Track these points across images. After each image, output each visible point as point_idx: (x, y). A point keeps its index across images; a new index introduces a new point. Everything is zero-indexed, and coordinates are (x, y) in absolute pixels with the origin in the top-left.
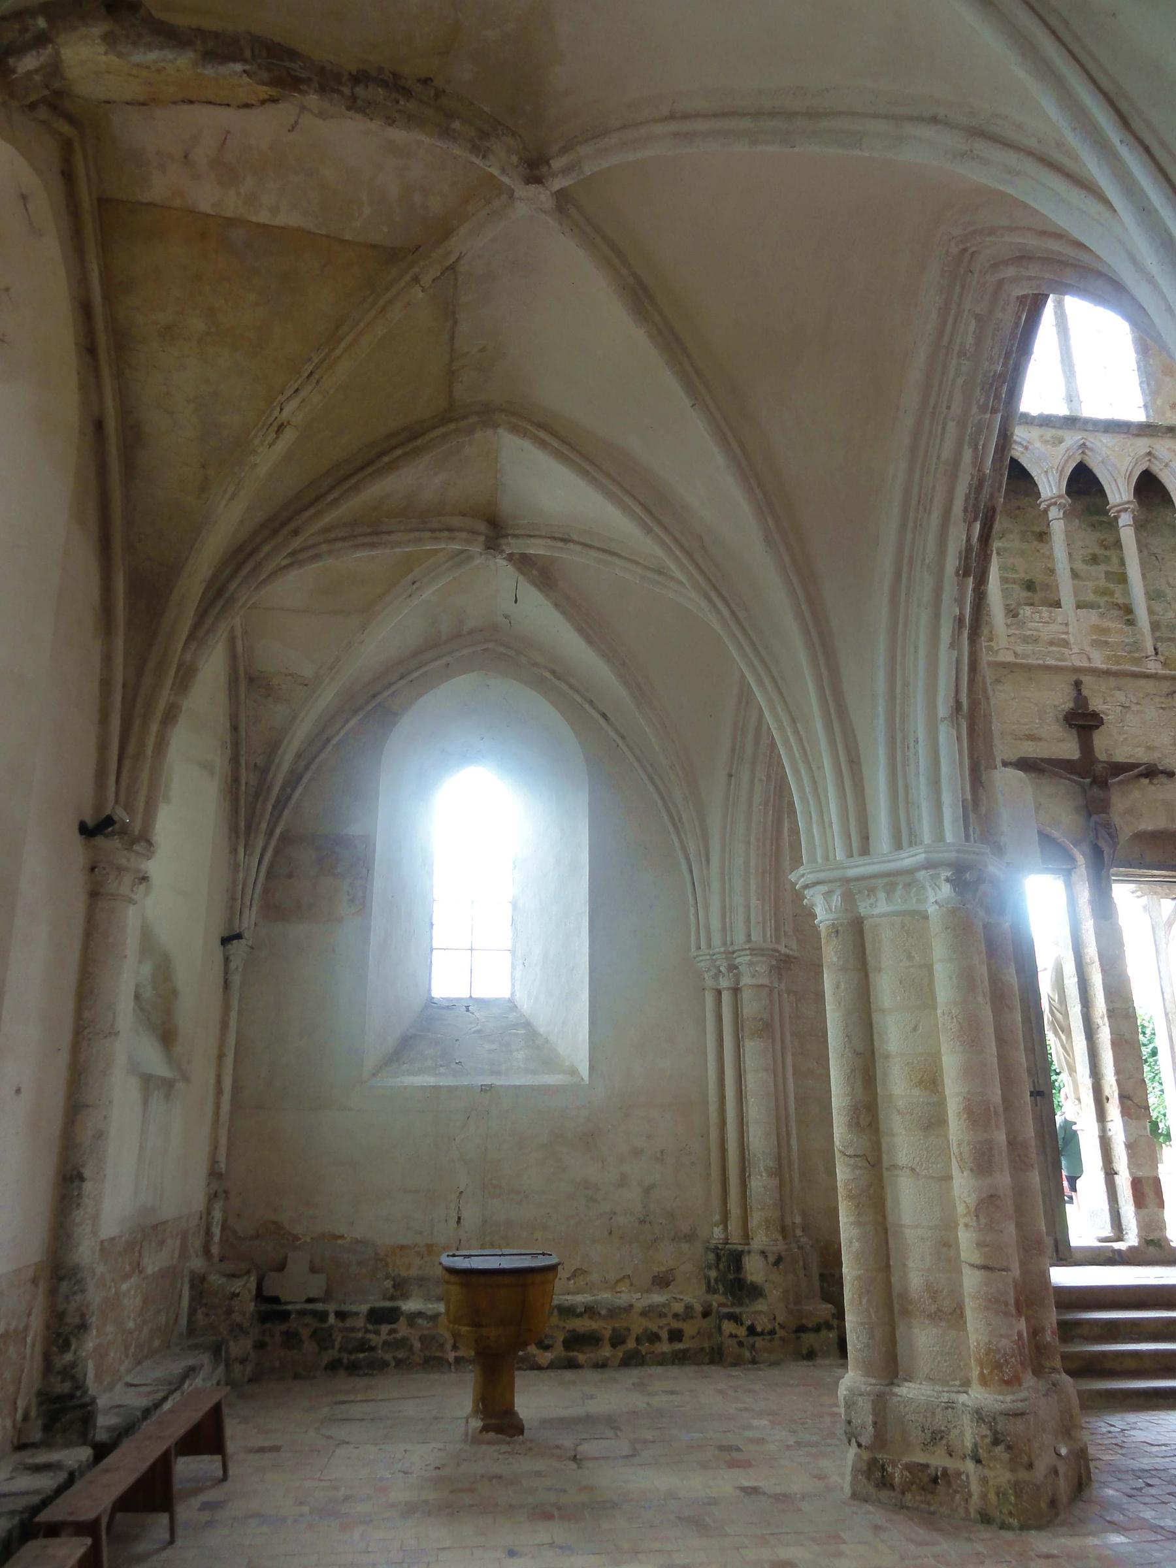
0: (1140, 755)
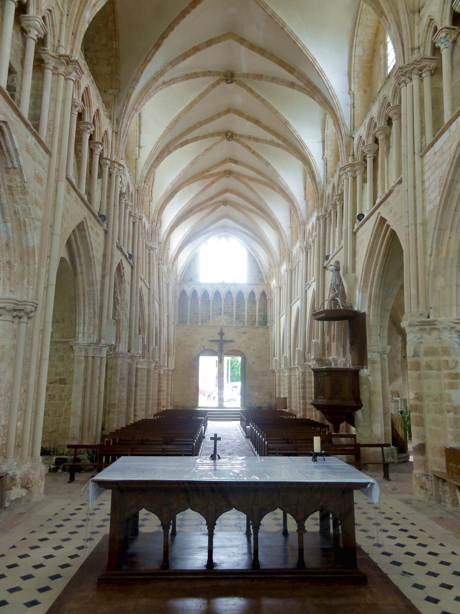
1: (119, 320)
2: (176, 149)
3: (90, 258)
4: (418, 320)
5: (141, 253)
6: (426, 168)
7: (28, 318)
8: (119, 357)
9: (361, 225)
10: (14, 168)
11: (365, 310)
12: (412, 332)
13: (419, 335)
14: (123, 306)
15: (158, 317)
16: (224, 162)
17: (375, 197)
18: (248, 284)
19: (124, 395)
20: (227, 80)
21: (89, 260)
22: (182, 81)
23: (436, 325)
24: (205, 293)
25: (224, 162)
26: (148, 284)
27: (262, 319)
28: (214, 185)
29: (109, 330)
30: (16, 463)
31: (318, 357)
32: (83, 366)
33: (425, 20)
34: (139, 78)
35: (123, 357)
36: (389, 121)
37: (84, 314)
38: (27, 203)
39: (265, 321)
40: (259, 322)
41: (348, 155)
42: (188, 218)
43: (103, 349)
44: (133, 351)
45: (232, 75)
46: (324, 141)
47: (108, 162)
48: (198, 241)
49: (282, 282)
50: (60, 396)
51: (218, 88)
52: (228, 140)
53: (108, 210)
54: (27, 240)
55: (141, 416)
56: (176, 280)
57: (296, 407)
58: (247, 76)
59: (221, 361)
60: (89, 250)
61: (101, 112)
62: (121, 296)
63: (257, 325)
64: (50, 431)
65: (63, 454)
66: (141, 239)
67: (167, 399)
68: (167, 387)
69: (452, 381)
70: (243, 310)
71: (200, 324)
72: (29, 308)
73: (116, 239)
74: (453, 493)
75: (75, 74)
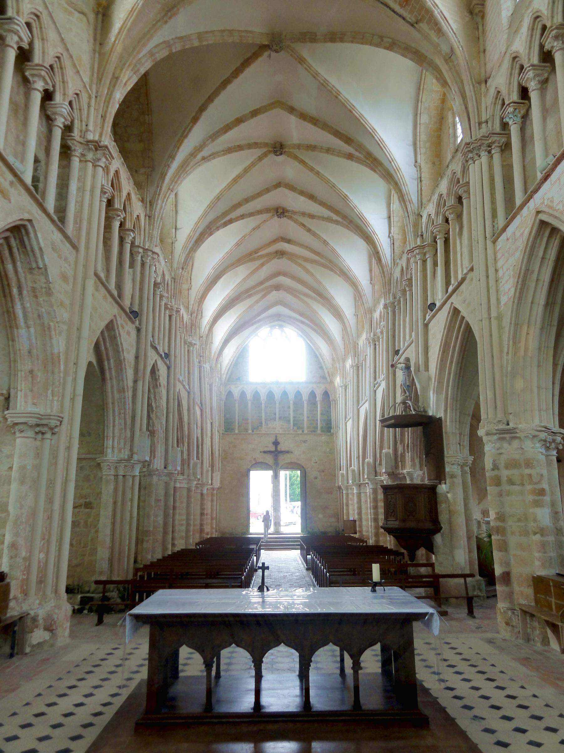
0: (287, 449)
1: (154, 431)
2: (218, 230)
3: (120, 361)
4: (496, 428)
5: (179, 351)
6: (499, 255)
7: (53, 434)
8: (154, 474)
9: (433, 316)
10: (39, 268)
11: (440, 414)
12: (490, 441)
13: (498, 445)
14: (158, 414)
15: (199, 425)
16: (275, 241)
17: (448, 283)
18: (306, 383)
19: (160, 519)
20: (275, 152)
21: (120, 364)
22: (224, 155)
23: (516, 433)
24: (256, 395)
25: (275, 241)
26: (187, 387)
27: (324, 424)
28: (265, 268)
29: (142, 443)
30: (38, 602)
31: (390, 470)
32: (112, 487)
33: (492, 92)
34: (175, 156)
35: (159, 475)
36: (460, 200)
37: (114, 426)
38: (51, 306)
39: (329, 428)
40: (322, 428)
41: (416, 236)
42: (234, 306)
43: (136, 466)
44: (170, 467)
45: (282, 146)
46: (389, 217)
47: (141, 250)
48: (246, 332)
49: (348, 380)
50: (86, 522)
51: (266, 160)
52: (279, 217)
53: (141, 304)
54: (52, 346)
55: (180, 545)
56: (220, 379)
57: (367, 531)
58: (299, 147)
59: (276, 477)
60: (119, 352)
61: (133, 196)
62: (155, 402)
63: (319, 431)
64: (73, 565)
65: (88, 592)
66: (178, 334)
67: (212, 523)
68: (212, 510)
69: (537, 498)
70: (302, 414)
71: (250, 431)
72: (53, 423)
73: (150, 338)
74: (542, 630)
75: (104, 160)
